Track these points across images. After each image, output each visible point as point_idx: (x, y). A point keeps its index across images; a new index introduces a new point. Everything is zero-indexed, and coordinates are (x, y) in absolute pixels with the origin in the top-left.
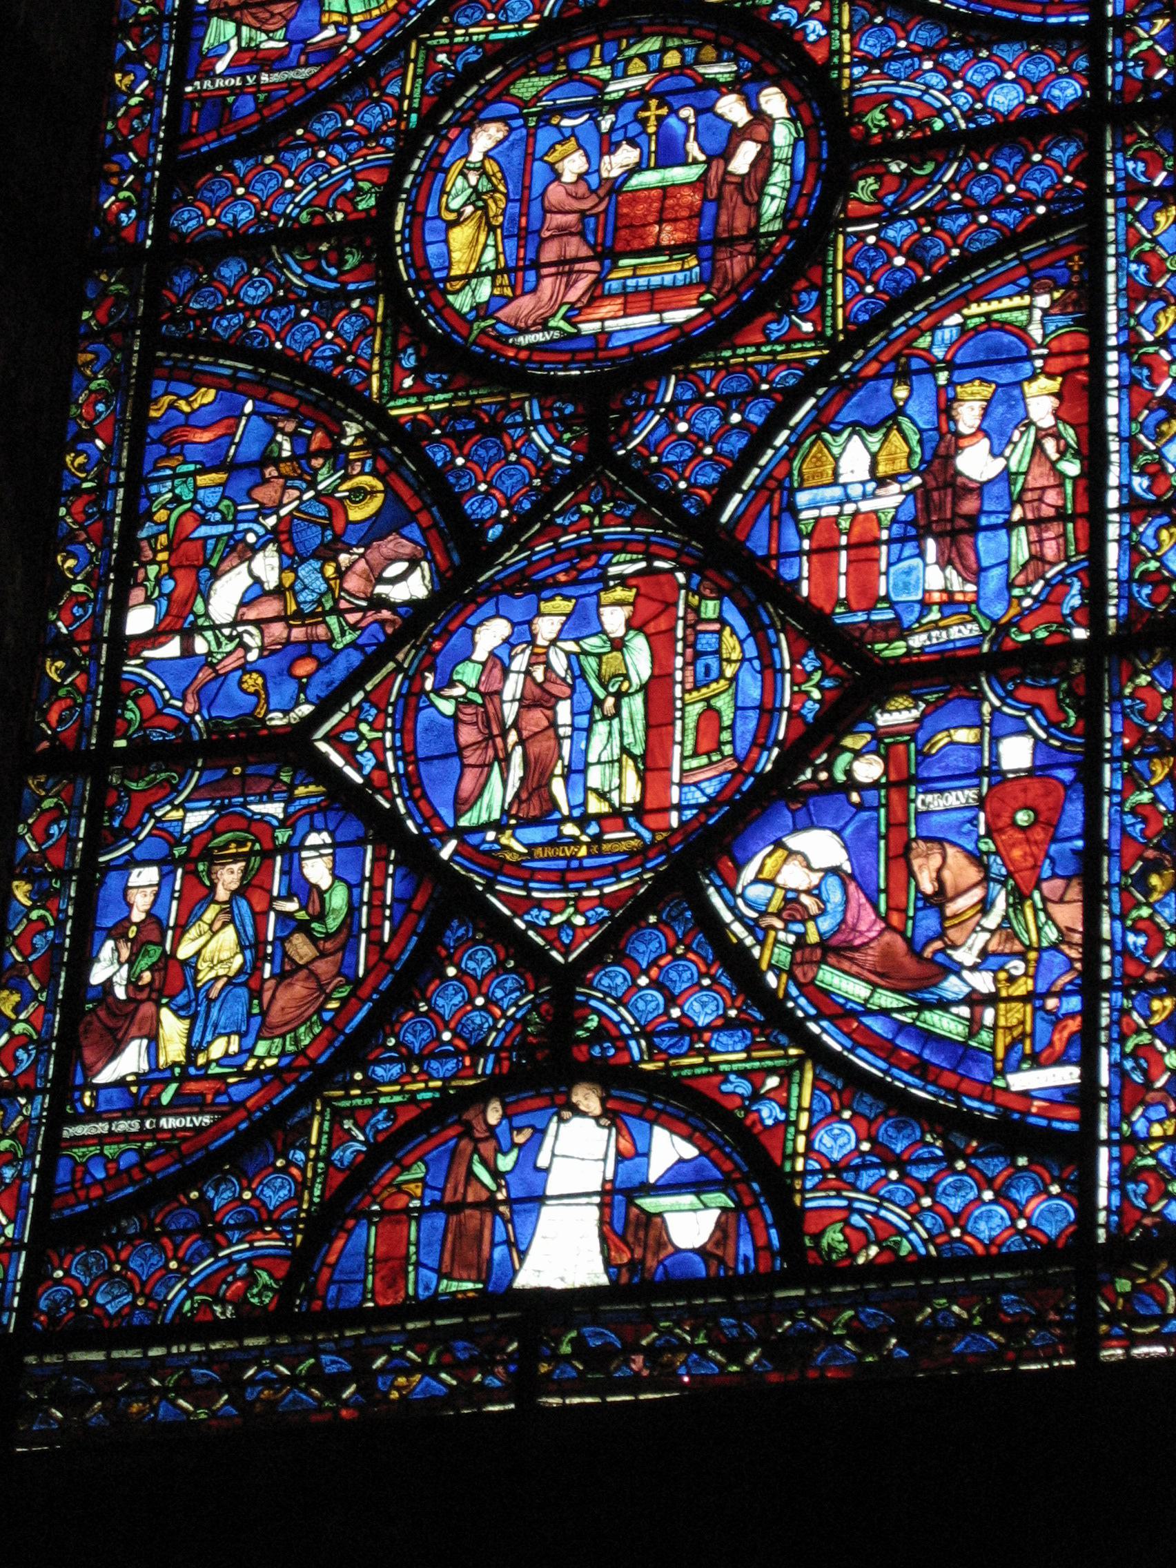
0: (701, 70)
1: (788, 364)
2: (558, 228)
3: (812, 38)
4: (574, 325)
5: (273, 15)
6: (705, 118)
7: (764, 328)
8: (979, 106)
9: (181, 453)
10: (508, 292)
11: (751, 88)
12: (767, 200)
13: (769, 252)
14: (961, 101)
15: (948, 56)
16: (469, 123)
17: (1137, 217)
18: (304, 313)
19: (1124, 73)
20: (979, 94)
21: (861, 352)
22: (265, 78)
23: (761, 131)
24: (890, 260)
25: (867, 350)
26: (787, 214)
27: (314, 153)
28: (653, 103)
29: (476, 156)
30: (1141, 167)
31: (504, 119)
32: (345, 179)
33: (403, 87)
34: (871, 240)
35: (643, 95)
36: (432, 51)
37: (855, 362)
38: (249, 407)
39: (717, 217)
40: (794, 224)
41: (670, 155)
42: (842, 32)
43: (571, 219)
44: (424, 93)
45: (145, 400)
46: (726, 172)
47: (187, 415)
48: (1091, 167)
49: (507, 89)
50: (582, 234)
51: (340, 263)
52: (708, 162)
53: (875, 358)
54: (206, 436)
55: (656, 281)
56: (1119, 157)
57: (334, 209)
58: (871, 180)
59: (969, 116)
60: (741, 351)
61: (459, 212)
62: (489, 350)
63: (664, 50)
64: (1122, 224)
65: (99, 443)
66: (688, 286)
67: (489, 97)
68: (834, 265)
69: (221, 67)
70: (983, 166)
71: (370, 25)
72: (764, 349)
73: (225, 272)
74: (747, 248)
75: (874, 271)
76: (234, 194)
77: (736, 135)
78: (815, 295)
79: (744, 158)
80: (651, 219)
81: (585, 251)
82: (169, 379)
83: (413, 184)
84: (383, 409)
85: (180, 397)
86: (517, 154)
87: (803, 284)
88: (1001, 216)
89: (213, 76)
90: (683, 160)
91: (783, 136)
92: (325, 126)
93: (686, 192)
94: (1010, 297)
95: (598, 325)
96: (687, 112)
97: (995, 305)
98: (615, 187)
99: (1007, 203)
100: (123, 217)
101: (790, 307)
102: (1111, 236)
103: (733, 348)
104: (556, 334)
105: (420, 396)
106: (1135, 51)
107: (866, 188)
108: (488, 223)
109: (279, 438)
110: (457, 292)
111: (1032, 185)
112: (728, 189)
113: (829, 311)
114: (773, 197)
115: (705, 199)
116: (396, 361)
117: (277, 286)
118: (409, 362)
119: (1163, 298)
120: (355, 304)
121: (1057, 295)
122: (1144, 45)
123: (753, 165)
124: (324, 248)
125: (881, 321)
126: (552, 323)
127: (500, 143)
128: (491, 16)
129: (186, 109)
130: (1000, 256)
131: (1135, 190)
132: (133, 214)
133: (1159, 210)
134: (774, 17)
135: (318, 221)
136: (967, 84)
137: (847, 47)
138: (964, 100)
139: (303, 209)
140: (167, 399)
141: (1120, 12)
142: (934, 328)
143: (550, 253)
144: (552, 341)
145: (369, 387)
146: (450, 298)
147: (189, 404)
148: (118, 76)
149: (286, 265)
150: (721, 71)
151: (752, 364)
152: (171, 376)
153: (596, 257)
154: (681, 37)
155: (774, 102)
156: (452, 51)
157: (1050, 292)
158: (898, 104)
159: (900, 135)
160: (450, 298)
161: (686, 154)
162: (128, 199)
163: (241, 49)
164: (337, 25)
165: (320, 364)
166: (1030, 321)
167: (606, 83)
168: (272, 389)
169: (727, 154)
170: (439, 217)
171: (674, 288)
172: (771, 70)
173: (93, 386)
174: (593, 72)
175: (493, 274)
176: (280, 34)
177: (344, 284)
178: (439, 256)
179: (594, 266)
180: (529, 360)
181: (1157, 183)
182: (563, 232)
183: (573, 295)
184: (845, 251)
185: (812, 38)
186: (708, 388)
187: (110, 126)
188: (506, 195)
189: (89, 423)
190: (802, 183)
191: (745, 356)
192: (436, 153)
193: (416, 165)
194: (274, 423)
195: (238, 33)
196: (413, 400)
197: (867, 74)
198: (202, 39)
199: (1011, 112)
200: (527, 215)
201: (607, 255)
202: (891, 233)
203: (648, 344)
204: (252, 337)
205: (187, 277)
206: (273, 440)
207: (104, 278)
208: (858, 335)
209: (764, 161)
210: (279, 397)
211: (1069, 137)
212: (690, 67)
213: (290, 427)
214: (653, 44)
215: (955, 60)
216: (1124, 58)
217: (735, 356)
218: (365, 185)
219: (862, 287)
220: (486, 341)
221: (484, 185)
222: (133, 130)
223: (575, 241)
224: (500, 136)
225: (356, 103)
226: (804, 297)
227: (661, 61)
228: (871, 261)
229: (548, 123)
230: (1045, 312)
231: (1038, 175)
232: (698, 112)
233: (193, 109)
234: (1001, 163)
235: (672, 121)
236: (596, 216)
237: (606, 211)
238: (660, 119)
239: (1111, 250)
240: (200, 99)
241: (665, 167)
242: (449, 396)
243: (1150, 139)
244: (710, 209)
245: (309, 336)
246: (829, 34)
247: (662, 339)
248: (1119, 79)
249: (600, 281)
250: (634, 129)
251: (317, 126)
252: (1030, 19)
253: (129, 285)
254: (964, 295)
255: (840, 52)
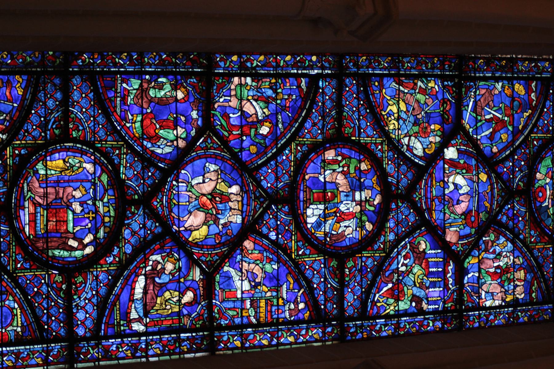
0: (102, 228)
1: (9, 261)
2: (59, 192)
3: (107, 259)
4: (28, 199)
5: (138, 99)
6: (87, 231)
7: (20, 254)
8: (79, 308)
9: (3, 86)
10: (41, 179)
11: (94, 243)
12: (59, 251)
13: (43, 253)
14: (81, 303)
15: (96, 298)
16: (95, 163)
17: (41, 353)
18: (42, 119)
19: (84, 346)
20: (83, 308)
21: (10, 281)
22: (119, 99)
23: (81, 247)
24: (36, 287)
25: (10, 283)
26: (54, 257)
27: (92, 117)
28: (94, 215)
29: (85, 165)
30: (55, 353)
31: (95, 173)
32: (83, 126)
33: (110, 141)
34: (43, 281)
35: (96, 212)
36: (120, 149)
37: (7, 279)
38: (15, 105)
39: (56, 237)
40: (50, 259)
41: (76, 222)
42: (108, 268)
43: (61, 195)
44: (107, 148)
45: (20, 74)
46: (69, 239)
47: (15, 87)
48: (57, 339)
49: (105, 172)
50: (56, 199)
51: (56, 128)
52: (74, 233)
53: (7, 285)
54: (8, 94)
55: (38, 222)
56: (59, 347)
57: (74, 124)
58: (61, 280)
59: (77, 305)
60: (14, 247)
61: (68, 162)
62: (24, 175)
63: (110, 217)
64: (39, 349)
65: (9, 61)
66: (35, 231)
67: (103, 167)
68: (37, 272)
69: (124, 85)
70: (61, 310)
71: (131, 129)
72: (14, 254)
73: (58, 94)
74: (45, 246)
75: (33, 283)
76: (83, 93)
77: (80, 241)
78: (28, 267)
79: (73, 243)
80: (58, 218)
81: (50, 200)
82: (27, 80)
83: (78, 147)
84: (9, 146)
85: (21, 84)
86: (84, 177)
87: (32, 264)
88: (45, 316)
89: (121, 84)
90: (74, 226)
91: (78, 253)
92: (101, 119)
93: (65, 228)
94: (21, 321)
95: (27, 206)
96: (90, 225)
97: (19, 316)
98: (69, 206)
99: (49, 316)
100: (80, 61)
101: (25, 261)
102: (36, 346)
103: (15, 246)
104: (26, 194)
105: (12, 156)
106: (90, 348)
107: (59, 279)
108: (63, 171)
109: (5, 115)
110: (43, 164)
111: (54, 324)
112: (64, 239)
113: (23, 271)
114: (59, 253)
115: (62, 233)
116: (23, 148)
117: (52, 110)
118: (23, 152)
119: (16, 362)
120: (43, 134)
121: (20, 333)
122: (92, 351)
123: (71, 246)
124: (62, 123)
125: (18, 286)
126: (29, 193)
127: (88, 172)
128: (128, 165)
129: (112, 76)
130: (34, 317)
131: (48, 352)
132: (81, 64)
133: (42, 359)
134: (116, 248)
135: (70, 119)
136: (86, 304)
137: (103, 269)
138: (82, 304)
139: (75, 115)
140: (21, 80)
141: (103, 344)
142: (14, 301)
143: (50, 190)
144: (24, 193)
145: (17, 141)
146: (41, 162)
147: (19, 87)
148: (126, 54)
149: (58, 112)
150: (101, 234)
151: (10, 251)
152: (28, 81)
153: (47, 204)
154: (113, 222)
155: (89, 250)
156: (119, 155)
157: (21, 331)
158: (83, 285)
159: (74, 286)
160: (41, 162)
161: (76, 227)
162: (85, 61)
163: (129, 91)
164: (132, 119)
165: (26, 125)
166: (13, 326)
167: (102, 201)
168: (20, 112)
169: (75, 239)
170: (67, 156)
171: (36, 226)
172: (98, 249)
173: (28, 58)
174: (106, 196)
175: (47, 174)
176: (132, 102)
177: (49, 130)
178: (55, 158)
179: (45, 204)
180: (19, 187)
181: (50, 358)
182: (57, 193)
183: (37, 198)
184: (40, 274)
185: (107, 259)
186: (4, 239)
187: (110, 53)
188: (71, 175)
189: (16, 58)
190: (63, 261)
191: (13, 249)
192: (87, 153)
193: (84, 147)
194: (9, 113)
195: (134, 89)
196: (11, 154)
197: (94, 276)
198: (134, 78)
199: (76, 317)
200: (64, 182)
201: (48, 207)
202: (44, 286)
203: (19, 221)
204: (37, 105)
205: (58, 82)
206: (4, 113)
207: (61, 57)
208: (14, 280)
209: (72, 249)
210: (18, 114)
211: (66, 333)
212: (104, 225)
213: (8, 118)
214: (112, 213)
215: (94, 300)
216: (89, 346)
217: (13, 246)
218: (80, 133)
219: (29, 280)
220: (26, 174)
221: (75, 168)
222: (107, 60)
223: (54, 197)
224: (90, 172)
225: (106, 128)
226: (28, 264)
227: (107, 216)
228: (37, 282)
229: (92, 185)
230: (15, 330)
231: (57, 325)
232: (89, 229)
233: (112, 78)
234: (61, 315)
235: (87, 221)
236: (61, 203)
237: (62, 205)
238: (89, 218)
239: (32, 347)
240: (114, 81)
241: (73, 221)
242: (11, 164)
243: (63, 355)
244: (58, 235)
245: (34, 121)
246: (107, 264)
247: (20, 225)
248: (82, 345)
249: (40, 205)
250: (86, 211)
251: (101, 116)
252: (104, 319)
253: (58, 65)
254: (24, 308)
255: (102, 267)
